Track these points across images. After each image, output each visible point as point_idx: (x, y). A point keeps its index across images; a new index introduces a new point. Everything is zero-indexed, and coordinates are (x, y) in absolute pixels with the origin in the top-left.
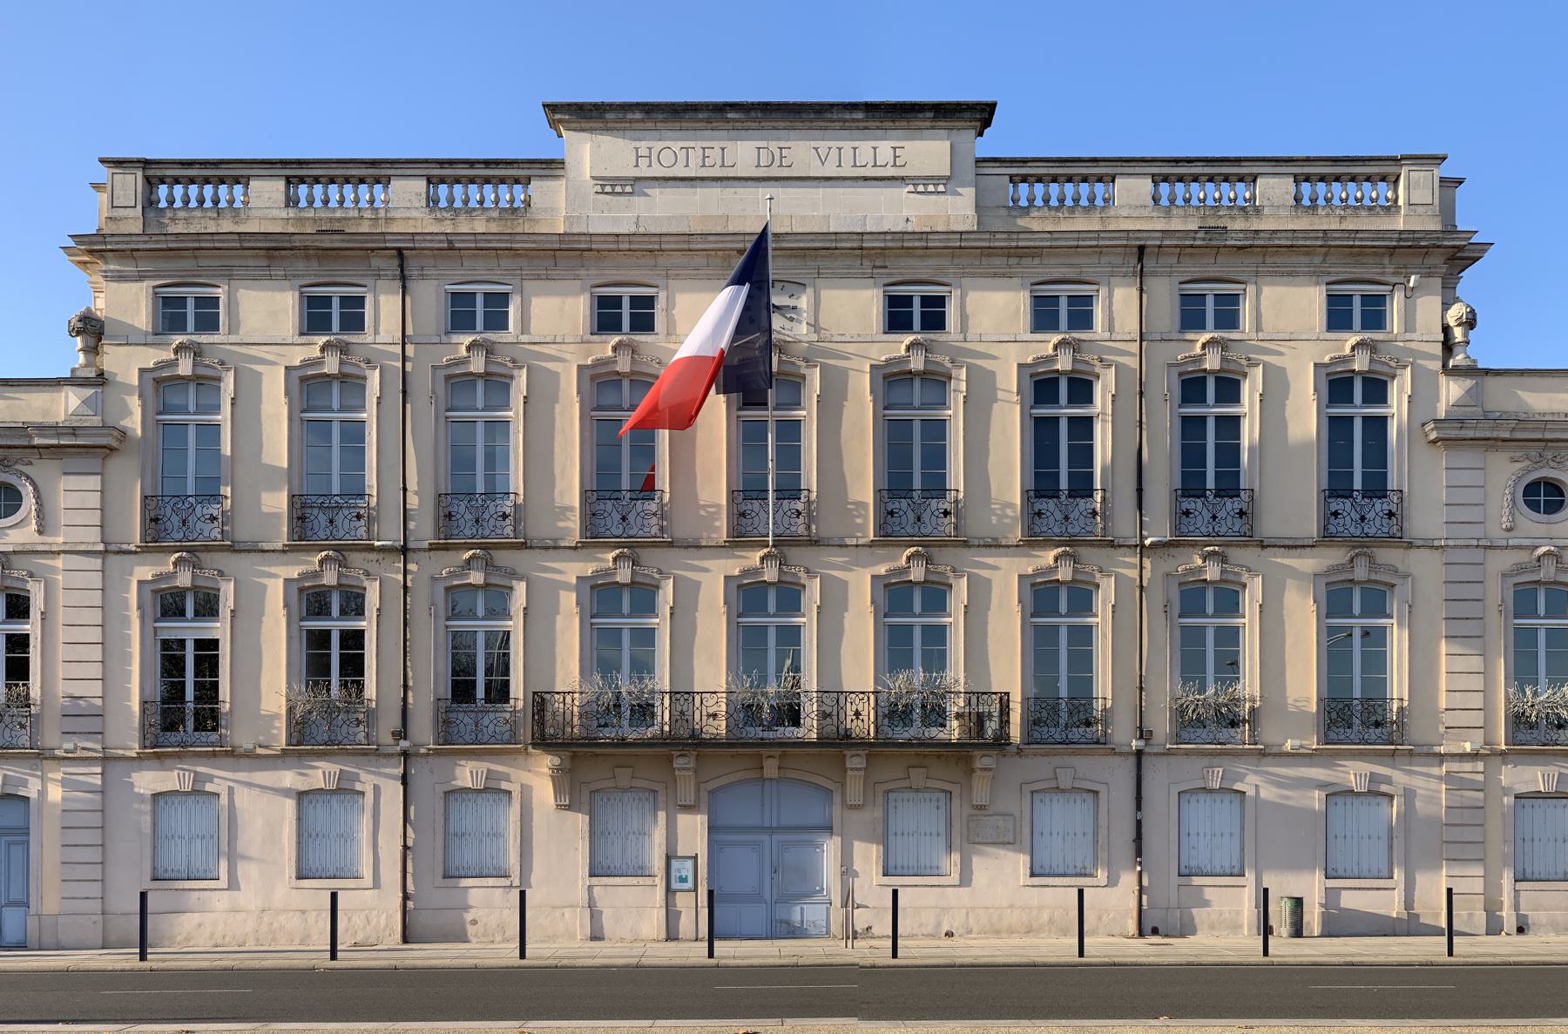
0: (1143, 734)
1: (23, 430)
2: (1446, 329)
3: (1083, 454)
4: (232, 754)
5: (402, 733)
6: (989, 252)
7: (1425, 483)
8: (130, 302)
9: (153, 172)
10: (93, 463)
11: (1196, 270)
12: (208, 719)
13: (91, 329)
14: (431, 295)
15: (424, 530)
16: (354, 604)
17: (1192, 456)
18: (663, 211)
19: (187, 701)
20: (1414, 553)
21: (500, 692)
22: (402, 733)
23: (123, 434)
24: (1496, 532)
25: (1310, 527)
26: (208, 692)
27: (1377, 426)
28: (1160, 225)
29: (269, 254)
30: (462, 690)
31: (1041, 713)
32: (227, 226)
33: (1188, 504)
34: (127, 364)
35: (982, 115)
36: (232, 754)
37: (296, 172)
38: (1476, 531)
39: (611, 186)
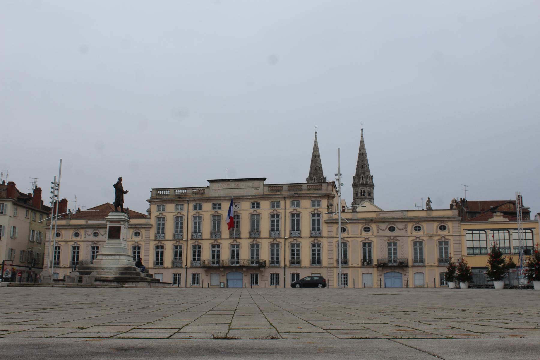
0: (285, 265)
1: (141, 225)
2: (328, 207)
3: (278, 225)
4: (164, 268)
5: (186, 265)
6: (264, 197)
7: (325, 228)
8: (154, 208)
9: (157, 190)
10: (148, 229)
11: (292, 200)
12: (162, 263)
13: (149, 211)
14: (191, 206)
15: (190, 237)
16: (181, 247)
17: (293, 225)
18: (221, 193)
19: (159, 261)
20: (324, 239)
21: (199, 260)
22: (186, 265)
23: (152, 225)
24: (335, 235)
25: (308, 235)
26: (162, 260)
27: (319, 220)
28: (288, 193)
29: (172, 201)
30: (194, 259)
31: (272, 262)
32: (166, 197)
33: (292, 232)
34: (154, 215)
35: (265, 179)
36: (164, 268)
37: (175, 189)
38: (332, 235)
39: (216, 190)
